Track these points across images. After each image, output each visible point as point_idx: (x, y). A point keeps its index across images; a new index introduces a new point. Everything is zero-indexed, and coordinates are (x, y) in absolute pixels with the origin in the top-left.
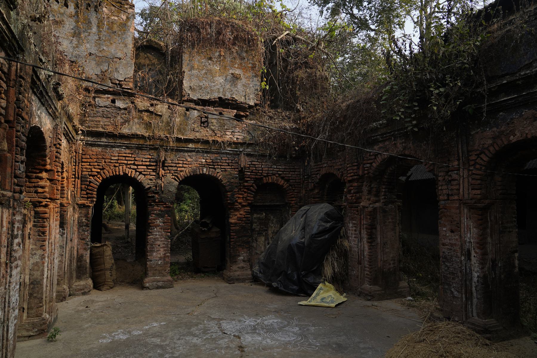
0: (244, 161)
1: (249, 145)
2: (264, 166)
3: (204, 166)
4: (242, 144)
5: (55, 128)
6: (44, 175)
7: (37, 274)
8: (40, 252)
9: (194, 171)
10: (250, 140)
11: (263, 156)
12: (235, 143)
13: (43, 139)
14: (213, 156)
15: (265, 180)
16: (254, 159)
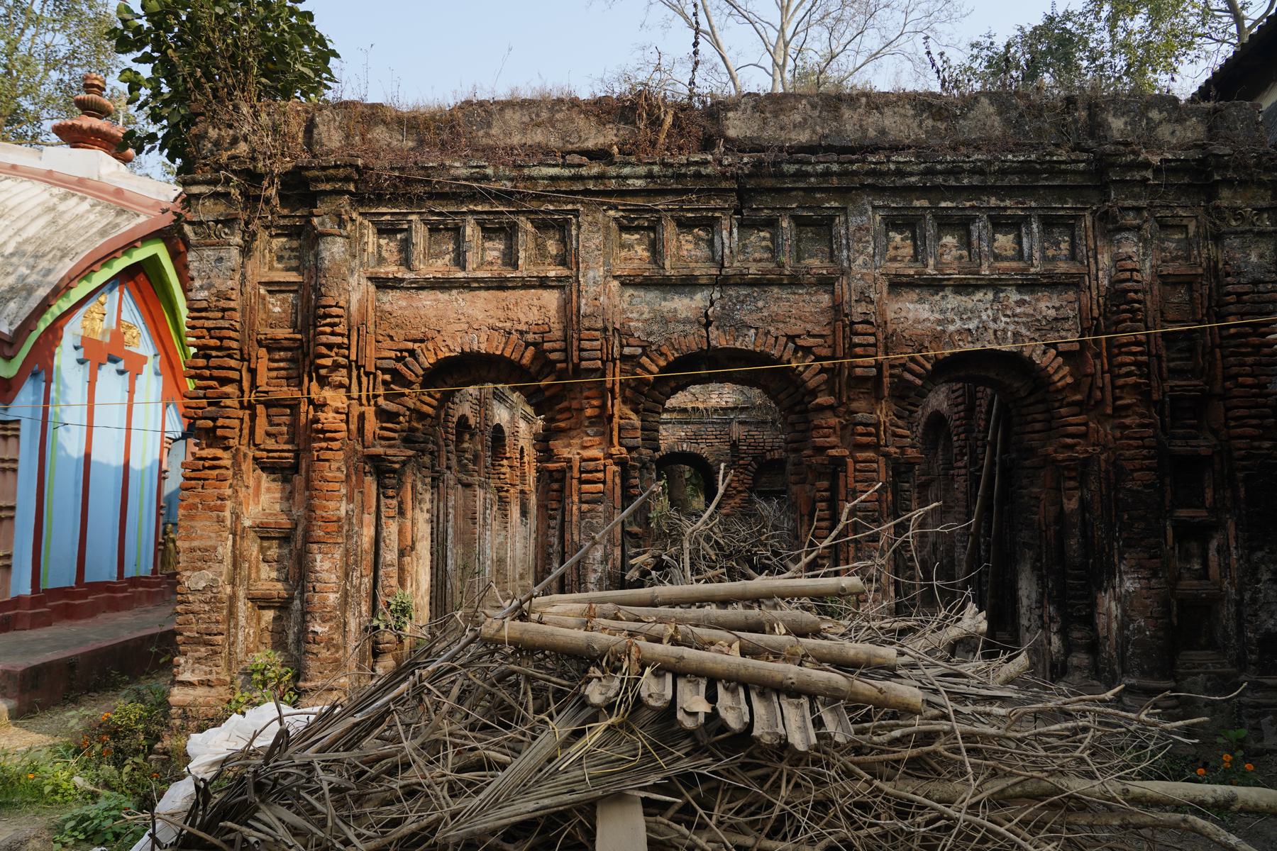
0: (737, 431)
1: (743, 410)
2: (766, 437)
3: (681, 440)
4: (733, 409)
5: (512, 418)
6: (505, 462)
7: (502, 552)
8: (504, 533)
9: (671, 447)
10: (744, 402)
11: (764, 422)
12: (722, 409)
13: (503, 432)
14: (694, 427)
15: (768, 456)
16: (752, 428)
